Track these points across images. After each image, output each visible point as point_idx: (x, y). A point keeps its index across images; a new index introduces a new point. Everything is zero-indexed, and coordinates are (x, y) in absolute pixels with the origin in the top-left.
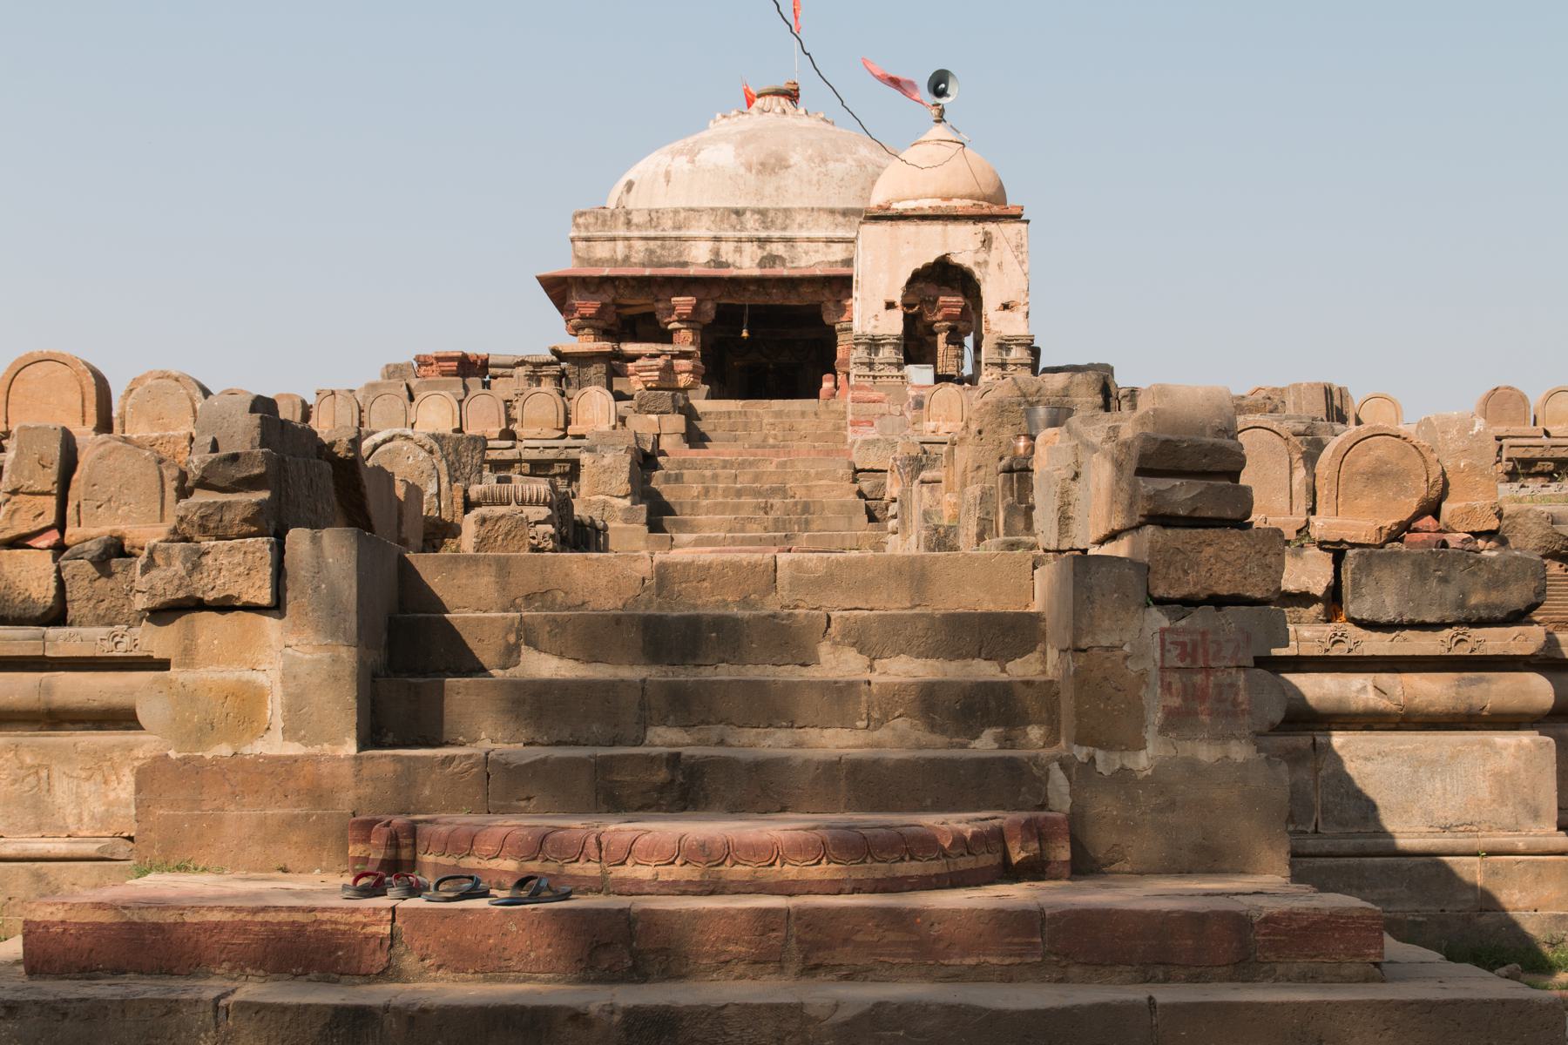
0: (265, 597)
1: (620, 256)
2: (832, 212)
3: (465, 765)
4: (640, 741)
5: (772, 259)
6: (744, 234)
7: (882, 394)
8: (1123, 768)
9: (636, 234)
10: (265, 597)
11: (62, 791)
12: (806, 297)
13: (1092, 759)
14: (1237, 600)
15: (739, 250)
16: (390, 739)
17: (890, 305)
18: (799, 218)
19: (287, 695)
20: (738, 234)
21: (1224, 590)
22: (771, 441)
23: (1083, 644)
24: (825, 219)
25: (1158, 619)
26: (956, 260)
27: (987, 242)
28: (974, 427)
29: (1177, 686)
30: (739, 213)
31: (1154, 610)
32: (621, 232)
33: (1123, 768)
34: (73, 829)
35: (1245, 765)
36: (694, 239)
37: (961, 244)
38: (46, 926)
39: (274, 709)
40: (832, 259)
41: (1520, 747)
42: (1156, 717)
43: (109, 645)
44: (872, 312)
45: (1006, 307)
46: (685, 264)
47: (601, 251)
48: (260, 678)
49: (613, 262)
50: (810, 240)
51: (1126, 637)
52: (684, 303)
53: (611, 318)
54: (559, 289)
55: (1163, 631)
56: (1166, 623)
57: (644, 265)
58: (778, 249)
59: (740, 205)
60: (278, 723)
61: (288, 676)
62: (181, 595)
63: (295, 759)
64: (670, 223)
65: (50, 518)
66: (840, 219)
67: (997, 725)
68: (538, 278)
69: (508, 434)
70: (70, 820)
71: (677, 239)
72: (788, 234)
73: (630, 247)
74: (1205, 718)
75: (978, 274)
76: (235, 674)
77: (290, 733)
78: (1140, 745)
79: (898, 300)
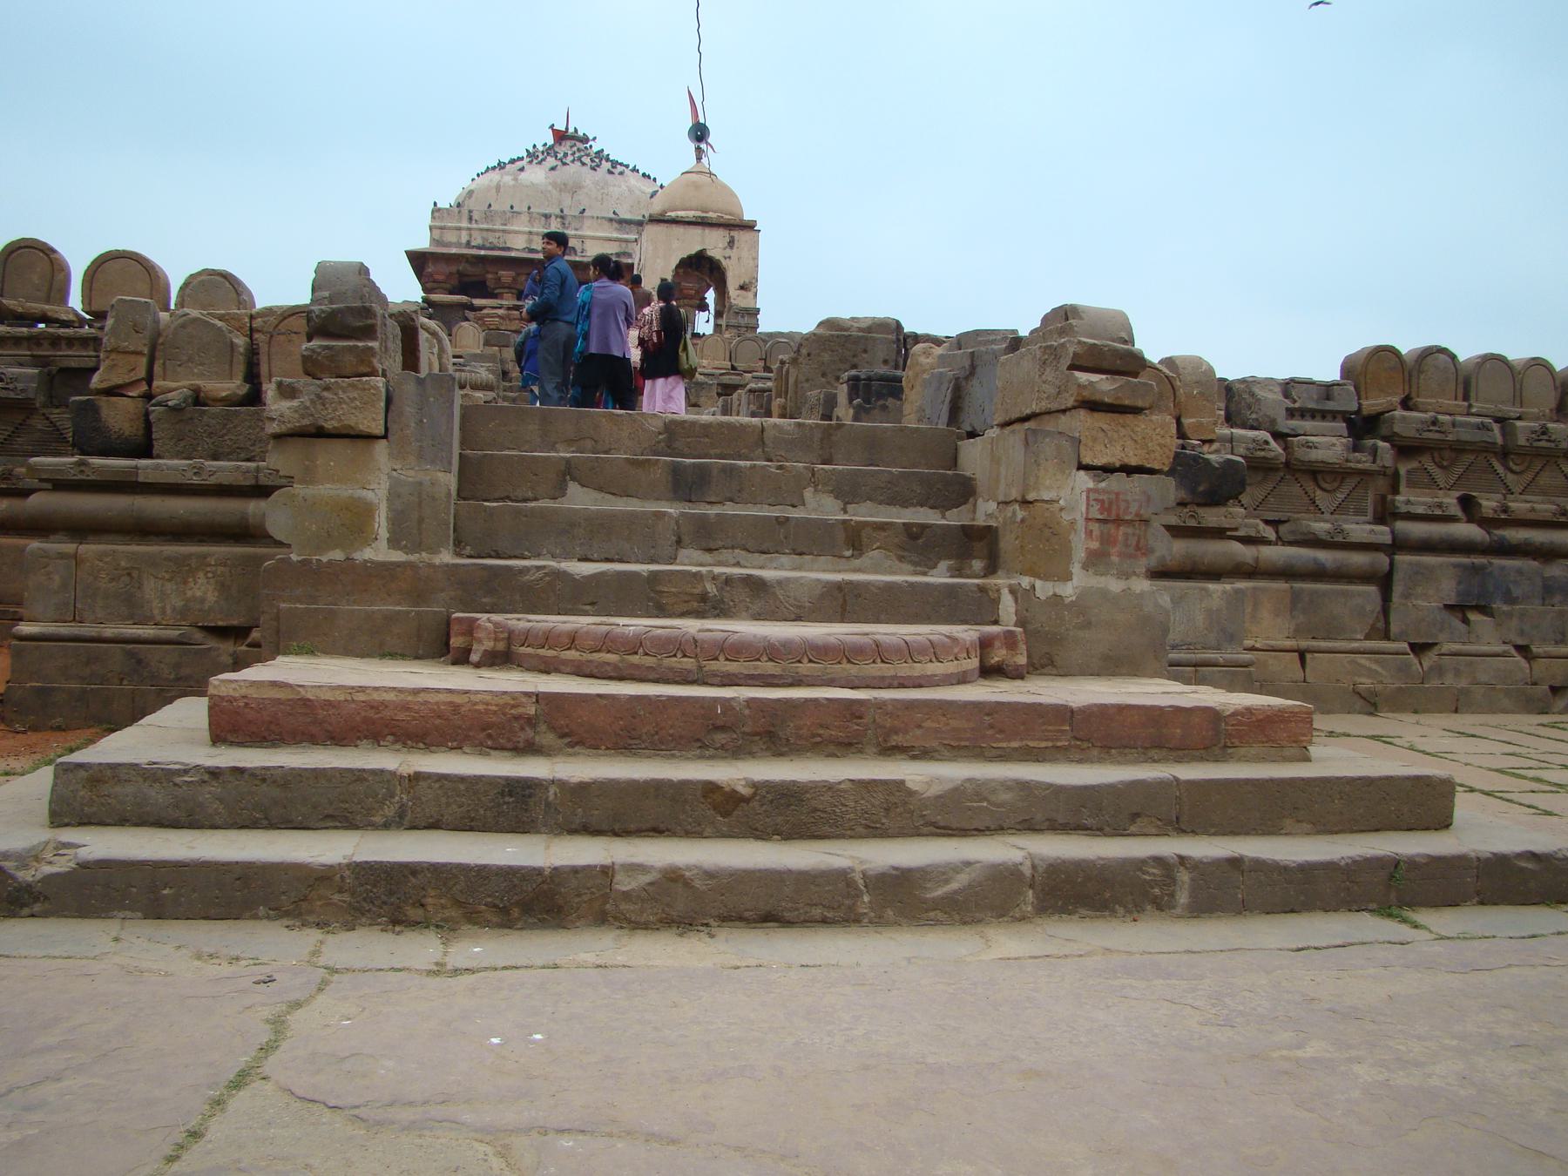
0: (380, 430)
1: (464, 240)
3: (539, 574)
4: (672, 560)
8: (1055, 595)
10: (380, 430)
11: (150, 588)
13: (1033, 587)
14: (1140, 470)
16: (468, 550)
18: (587, 223)
19: (390, 509)
21: (1133, 462)
23: (1030, 497)
24: (607, 224)
25: (1084, 480)
26: (710, 253)
27: (731, 243)
28: (804, 351)
29: (1096, 533)
31: (1082, 473)
32: (465, 224)
33: (1055, 595)
34: (158, 618)
35: (1142, 595)
37: (713, 243)
38: (231, 700)
39: (381, 524)
41: (1224, 592)
42: (1079, 554)
43: (189, 474)
45: (742, 288)
46: (509, 249)
47: (451, 237)
48: (369, 495)
49: (459, 245)
51: (1062, 494)
52: (506, 275)
53: (455, 282)
54: (419, 260)
55: (1089, 491)
56: (1091, 485)
57: (479, 248)
60: (384, 533)
61: (393, 495)
62: (306, 422)
63: (398, 565)
65: (142, 373)
66: (615, 225)
67: (949, 558)
70: (156, 612)
71: (504, 231)
74: (1115, 559)
75: (724, 263)
76: (345, 491)
77: (394, 543)
78: (1068, 577)
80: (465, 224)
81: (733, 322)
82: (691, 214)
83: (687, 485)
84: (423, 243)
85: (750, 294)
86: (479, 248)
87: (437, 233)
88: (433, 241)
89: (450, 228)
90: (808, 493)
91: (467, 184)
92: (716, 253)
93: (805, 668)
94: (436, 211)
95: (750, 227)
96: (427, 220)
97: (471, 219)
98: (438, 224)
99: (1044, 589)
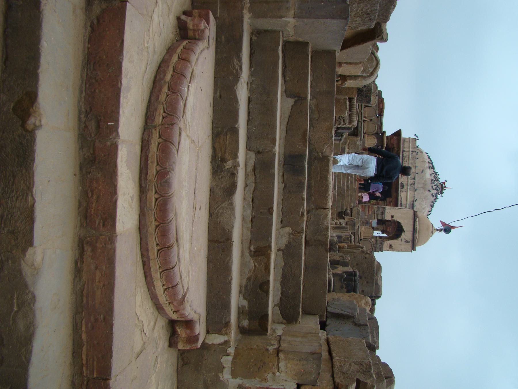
1: (405, 149)
3: (237, 67)
5: (403, 186)
8: (224, 368)
12: (394, 194)
13: (228, 355)
16: (255, 38)
17: (392, 217)
18: (412, 193)
23: (281, 355)
24: (412, 200)
26: (403, 234)
27: (407, 242)
28: (367, 256)
32: (411, 150)
33: (224, 368)
37: (407, 235)
44: (391, 212)
45: (391, 246)
47: (406, 145)
49: (404, 148)
51: (283, 374)
54: (398, 134)
57: (403, 155)
58: (405, 187)
66: (412, 203)
67: (249, 306)
68: (400, 130)
75: (400, 239)
78: (234, 376)
79: (394, 219)
80: (411, 150)
81: (378, 242)
82: (418, 227)
83: (292, 163)
84: (404, 135)
85: (388, 249)
86: (403, 155)
87: (408, 140)
88: (405, 139)
89: (409, 144)
90: (288, 230)
91: (425, 151)
92: (404, 236)
93: (152, 196)
95: (413, 249)
97: (413, 152)
98: (411, 140)
99: (227, 361)
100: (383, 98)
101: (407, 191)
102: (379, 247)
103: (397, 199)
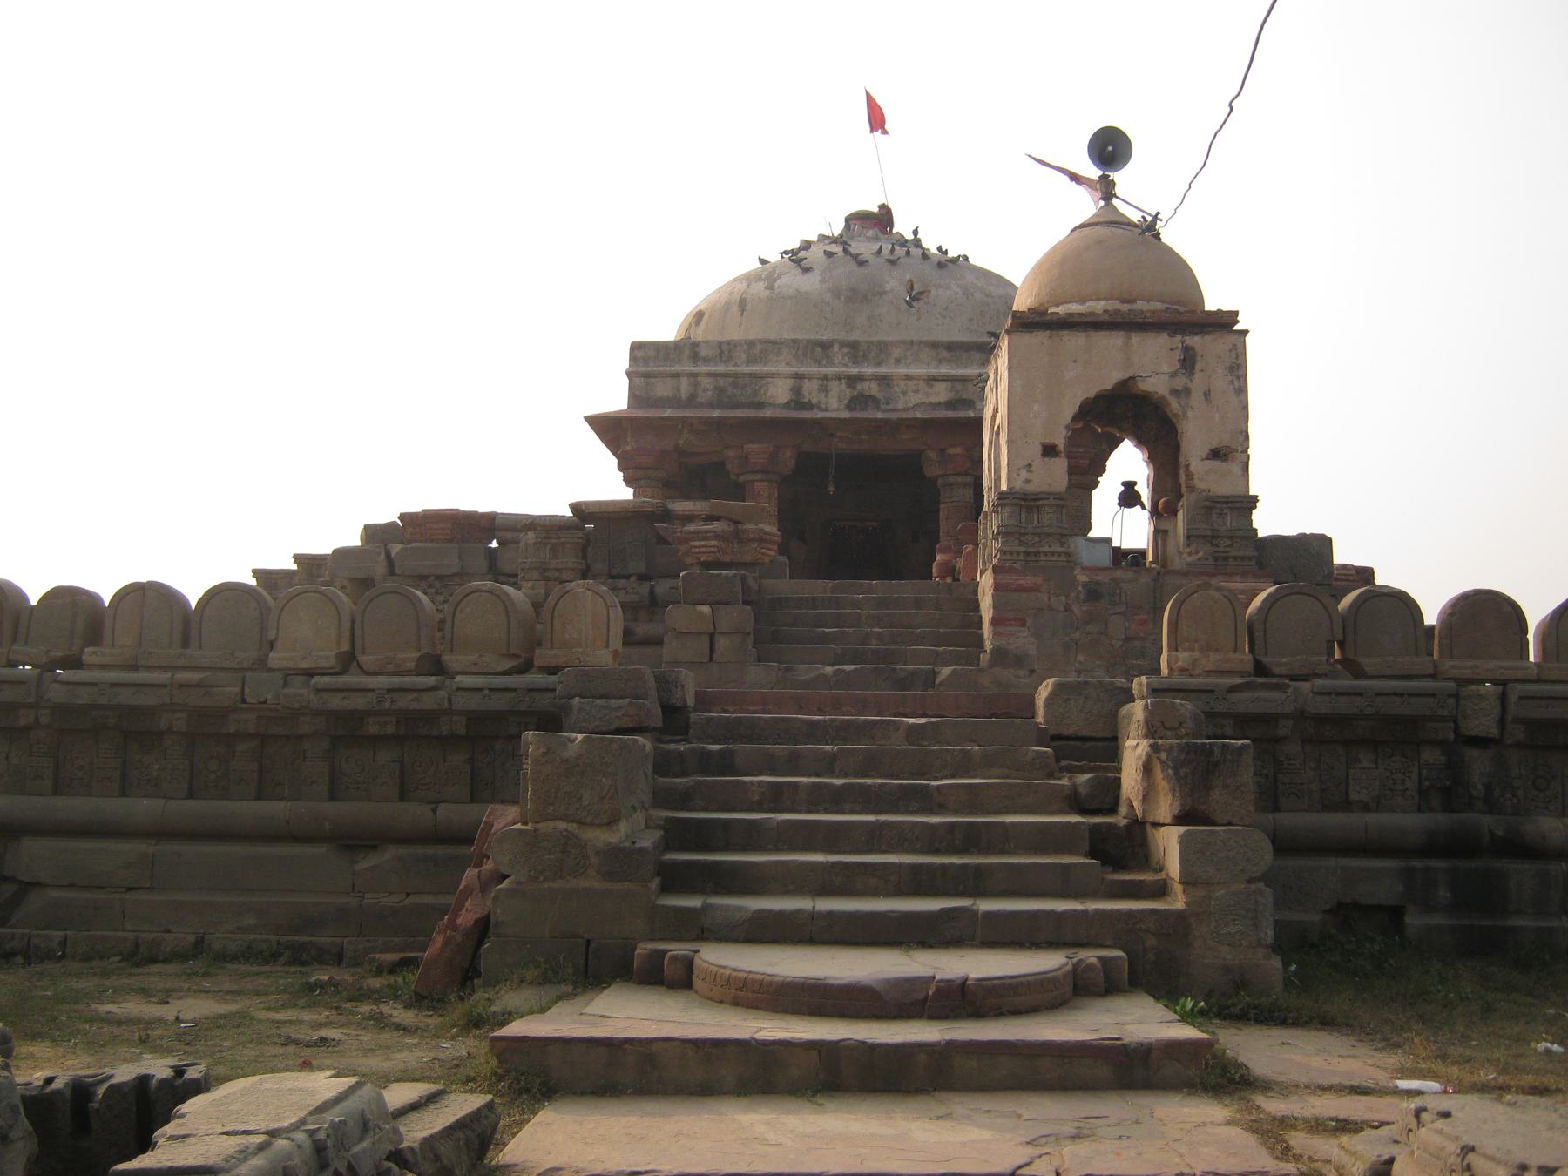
2: (934, 345)
6: (829, 370)
7: (1039, 580)
9: (704, 369)
15: (824, 390)
17: (1049, 451)
18: (896, 353)
20: (824, 370)
22: (874, 645)
27: (1188, 361)
30: (826, 346)
32: (689, 368)
36: (772, 375)
37: (1150, 363)
40: (934, 399)
45: (1216, 454)
46: (761, 405)
47: (662, 389)
49: (675, 402)
50: (908, 377)
52: (757, 451)
57: (711, 406)
58: (872, 388)
59: (826, 336)
64: (744, 356)
66: (945, 354)
69: (435, 666)
72: (883, 370)
73: (696, 385)
75: (1174, 405)
79: (1060, 441)
82: (1098, 306)
84: (616, 399)
85: (1236, 468)
92: (1156, 384)
94: (637, 348)
95: (1225, 322)
96: (624, 362)
98: (642, 369)
100: (403, 517)
101: (885, 380)
102: (1230, 521)
103: (927, 425)
